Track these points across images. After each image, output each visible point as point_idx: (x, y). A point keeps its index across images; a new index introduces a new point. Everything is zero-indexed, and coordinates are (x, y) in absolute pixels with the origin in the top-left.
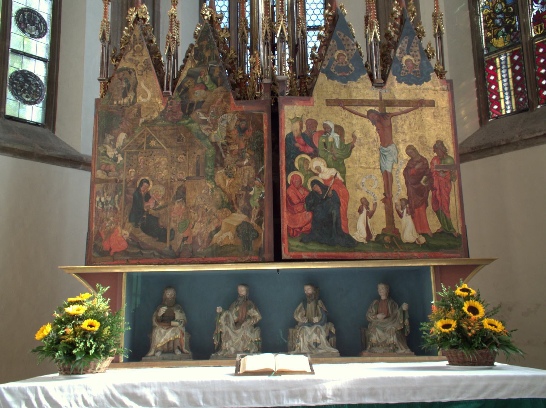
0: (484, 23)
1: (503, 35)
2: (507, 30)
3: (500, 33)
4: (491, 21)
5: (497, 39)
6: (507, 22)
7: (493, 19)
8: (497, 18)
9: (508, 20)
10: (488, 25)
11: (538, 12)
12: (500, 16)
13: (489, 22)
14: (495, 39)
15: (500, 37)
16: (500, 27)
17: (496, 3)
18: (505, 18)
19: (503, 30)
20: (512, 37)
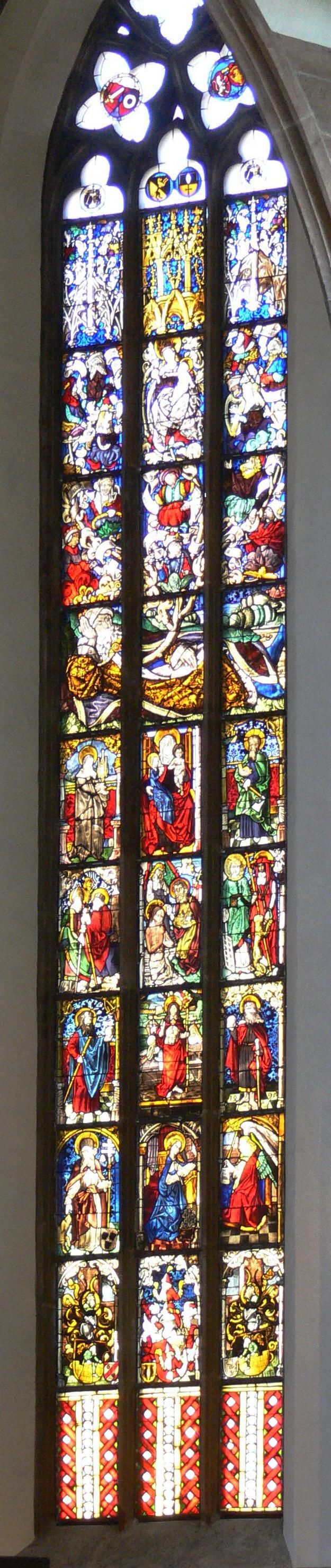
0: (62, 1323)
1: (92, 1360)
2: (100, 1355)
3: (87, 1355)
4: (74, 1323)
5: (81, 1363)
6: (99, 1336)
7: (80, 1321)
8: (84, 1321)
9: (102, 1334)
10: (70, 1330)
11: (149, 1338)
12: (90, 1319)
13: (71, 1322)
14: (78, 1362)
15: (86, 1361)
16: (88, 1342)
17: (86, 1290)
18: (98, 1328)
19: (93, 1349)
20: (106, 1370)
